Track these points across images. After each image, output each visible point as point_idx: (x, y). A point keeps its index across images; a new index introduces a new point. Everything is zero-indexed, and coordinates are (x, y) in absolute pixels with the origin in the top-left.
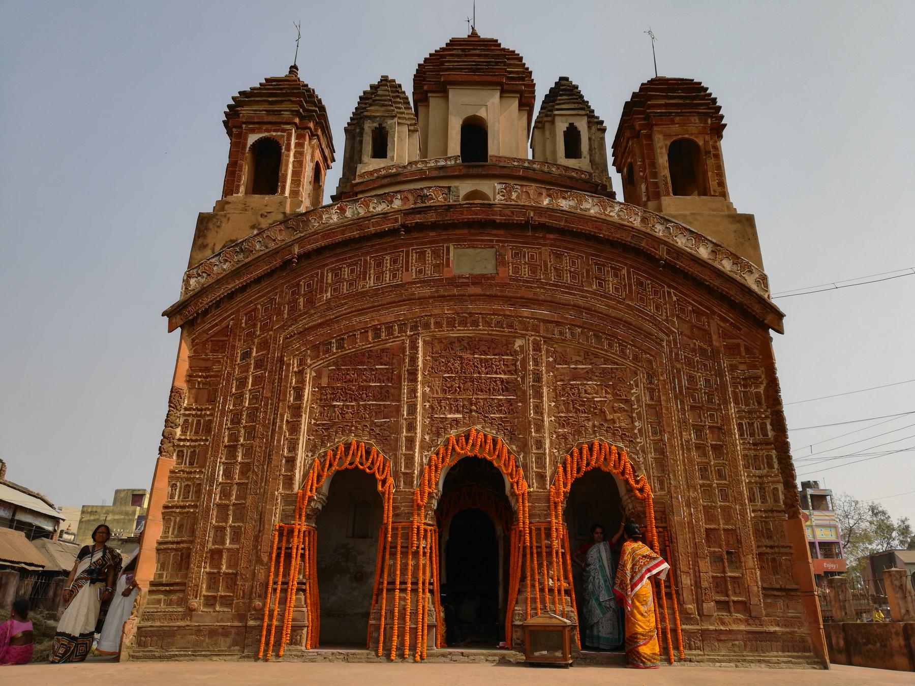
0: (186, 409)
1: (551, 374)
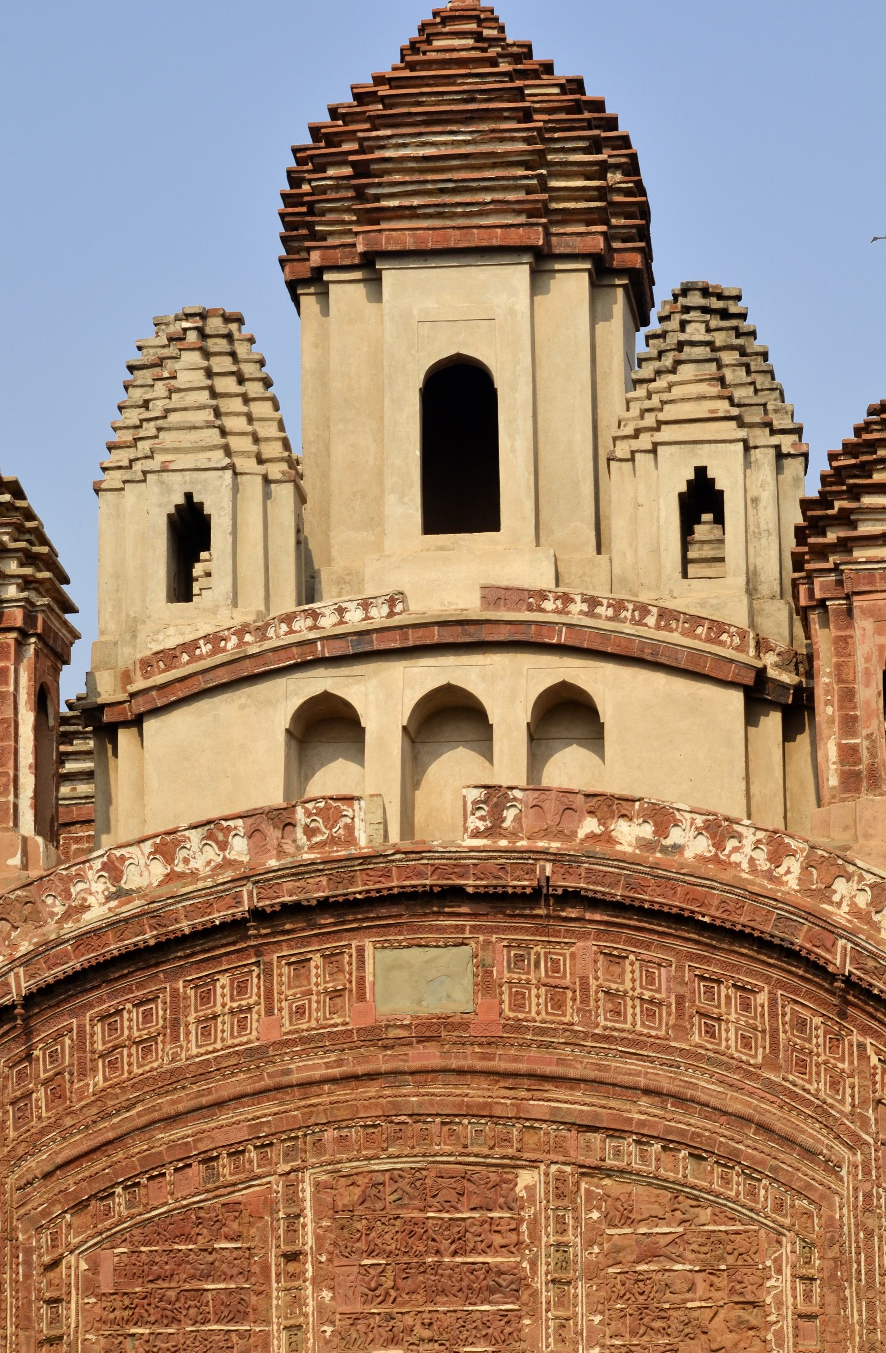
1: (596, 1249)
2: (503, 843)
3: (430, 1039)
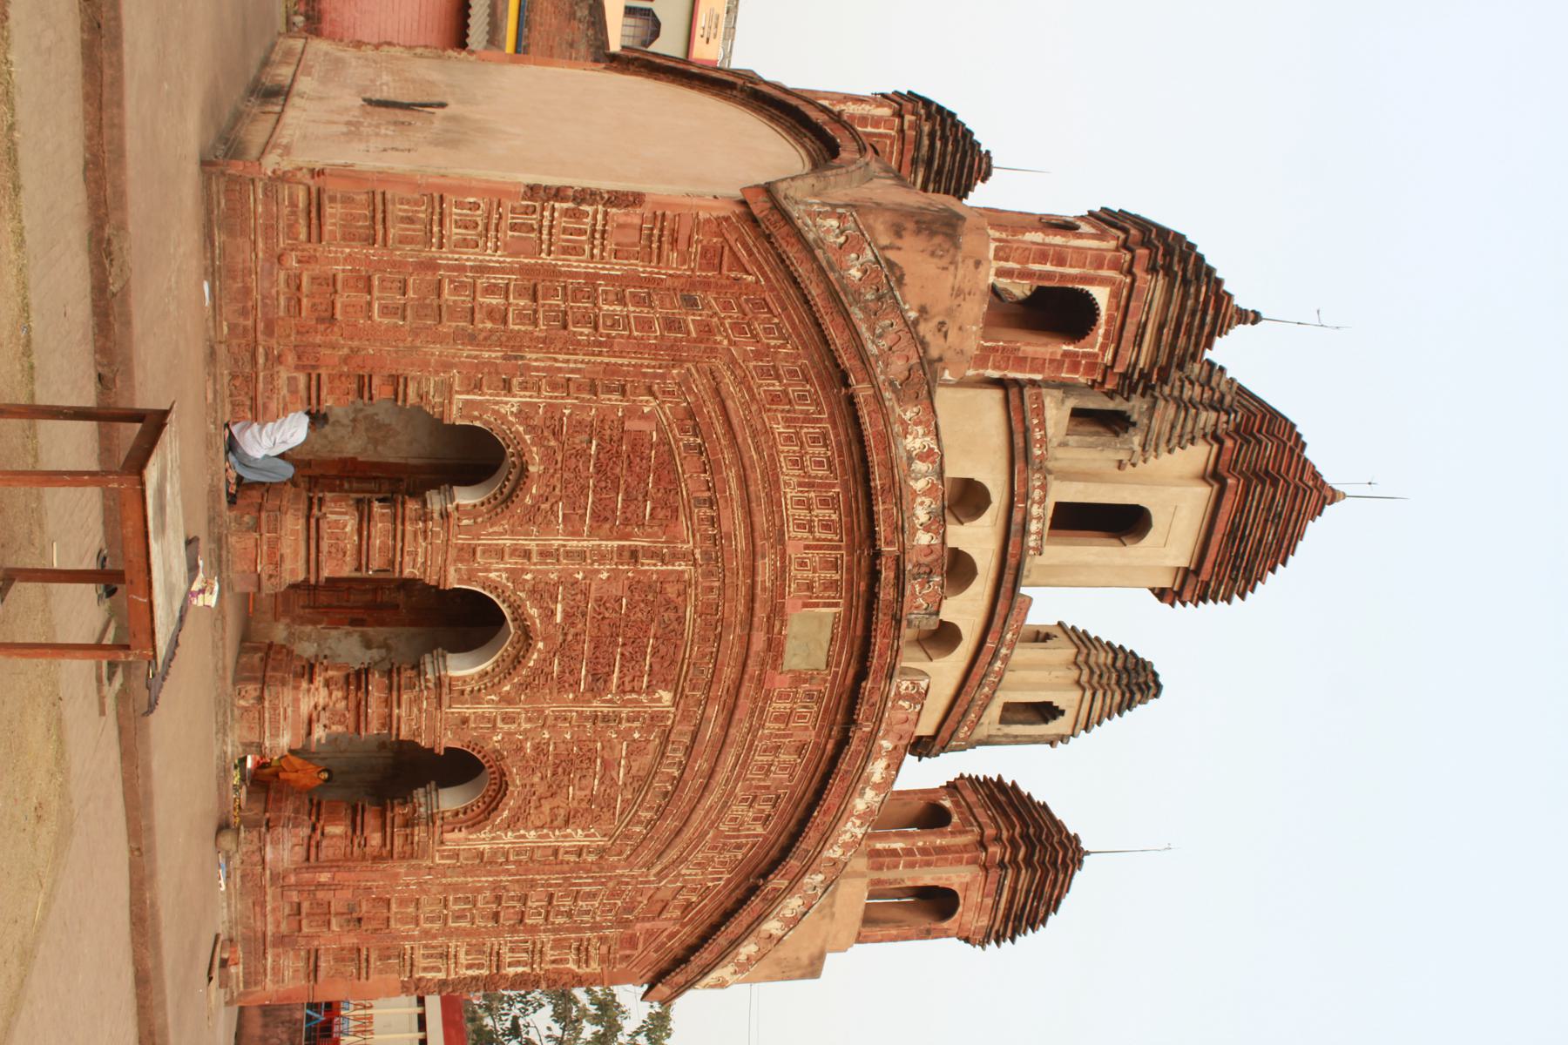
3: (769, 645)
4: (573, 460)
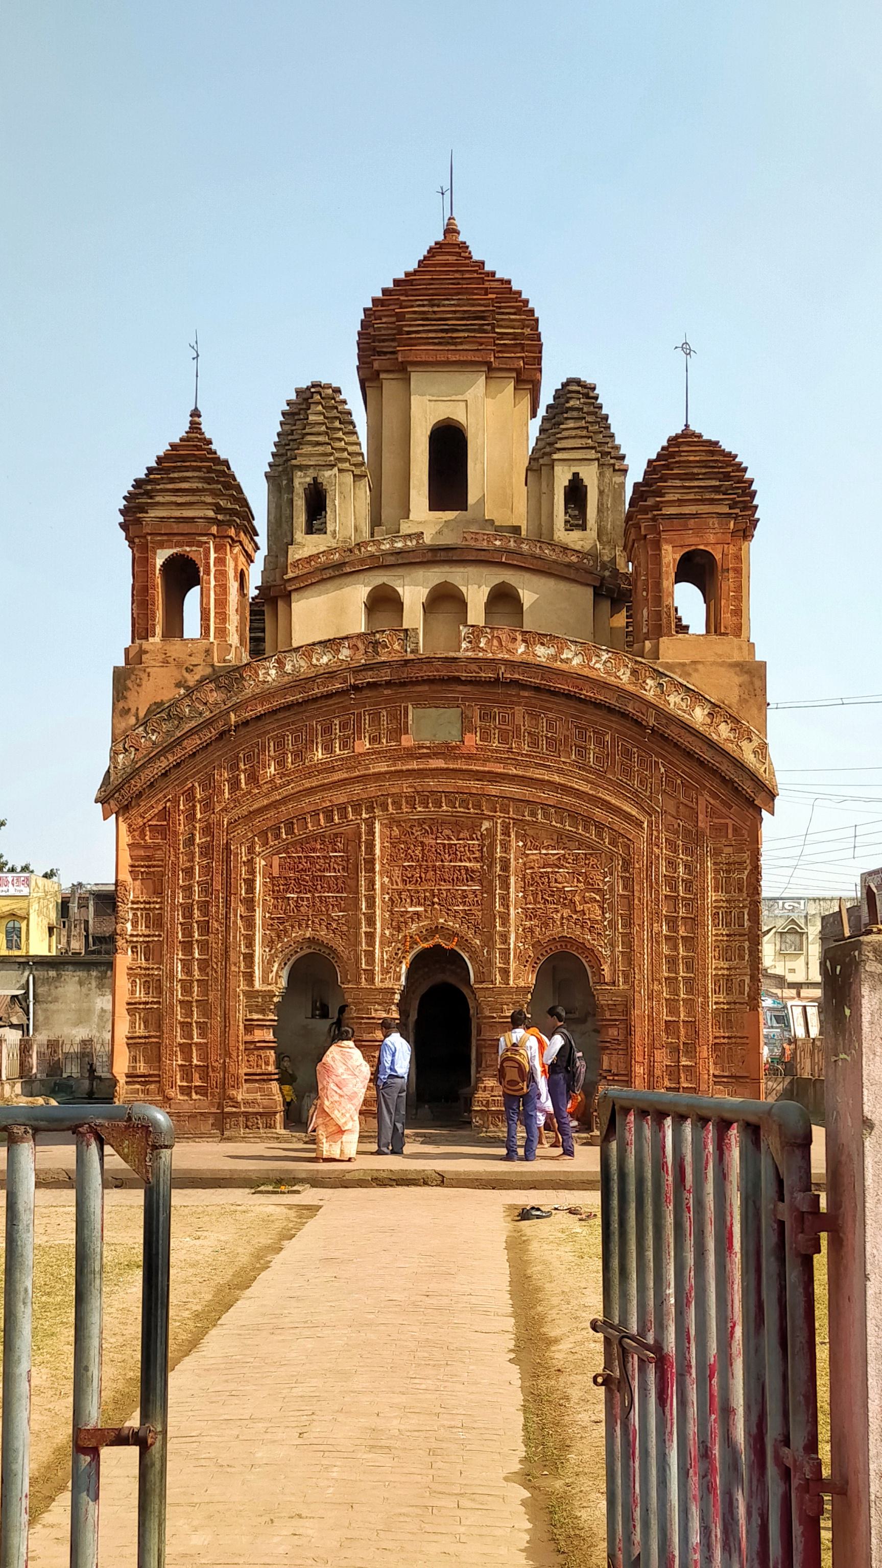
0: (133, 903)
2: (481, 654)
4: (302, 908)
